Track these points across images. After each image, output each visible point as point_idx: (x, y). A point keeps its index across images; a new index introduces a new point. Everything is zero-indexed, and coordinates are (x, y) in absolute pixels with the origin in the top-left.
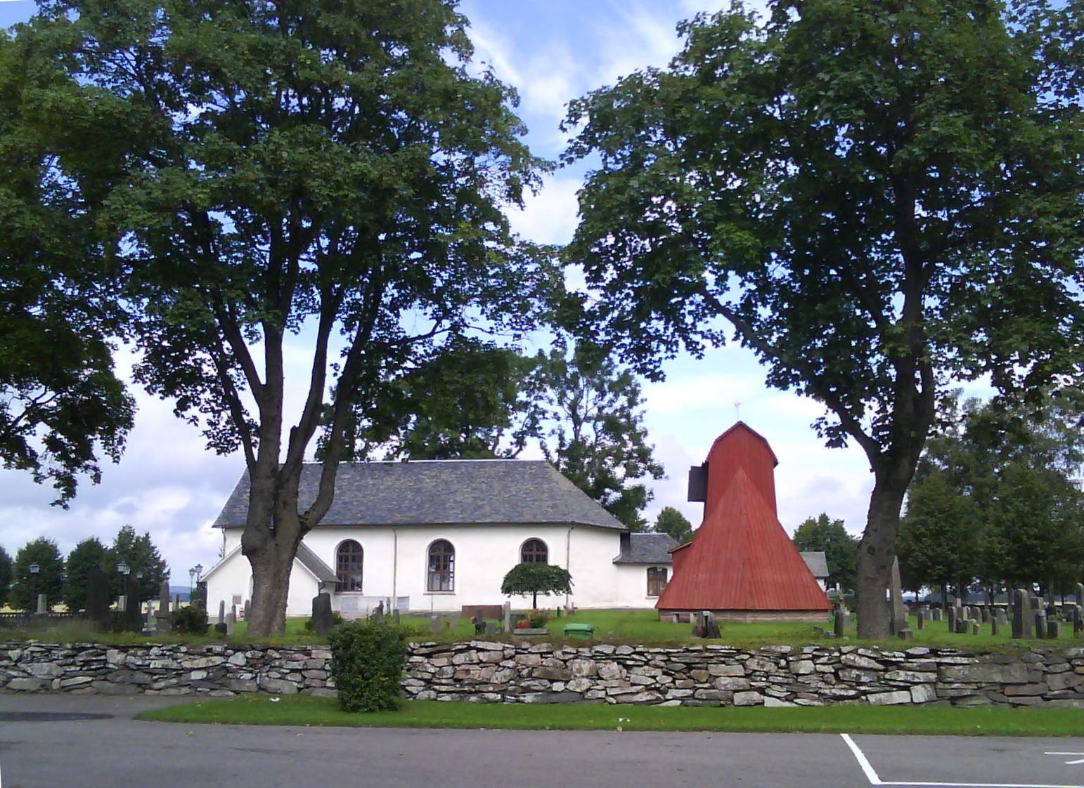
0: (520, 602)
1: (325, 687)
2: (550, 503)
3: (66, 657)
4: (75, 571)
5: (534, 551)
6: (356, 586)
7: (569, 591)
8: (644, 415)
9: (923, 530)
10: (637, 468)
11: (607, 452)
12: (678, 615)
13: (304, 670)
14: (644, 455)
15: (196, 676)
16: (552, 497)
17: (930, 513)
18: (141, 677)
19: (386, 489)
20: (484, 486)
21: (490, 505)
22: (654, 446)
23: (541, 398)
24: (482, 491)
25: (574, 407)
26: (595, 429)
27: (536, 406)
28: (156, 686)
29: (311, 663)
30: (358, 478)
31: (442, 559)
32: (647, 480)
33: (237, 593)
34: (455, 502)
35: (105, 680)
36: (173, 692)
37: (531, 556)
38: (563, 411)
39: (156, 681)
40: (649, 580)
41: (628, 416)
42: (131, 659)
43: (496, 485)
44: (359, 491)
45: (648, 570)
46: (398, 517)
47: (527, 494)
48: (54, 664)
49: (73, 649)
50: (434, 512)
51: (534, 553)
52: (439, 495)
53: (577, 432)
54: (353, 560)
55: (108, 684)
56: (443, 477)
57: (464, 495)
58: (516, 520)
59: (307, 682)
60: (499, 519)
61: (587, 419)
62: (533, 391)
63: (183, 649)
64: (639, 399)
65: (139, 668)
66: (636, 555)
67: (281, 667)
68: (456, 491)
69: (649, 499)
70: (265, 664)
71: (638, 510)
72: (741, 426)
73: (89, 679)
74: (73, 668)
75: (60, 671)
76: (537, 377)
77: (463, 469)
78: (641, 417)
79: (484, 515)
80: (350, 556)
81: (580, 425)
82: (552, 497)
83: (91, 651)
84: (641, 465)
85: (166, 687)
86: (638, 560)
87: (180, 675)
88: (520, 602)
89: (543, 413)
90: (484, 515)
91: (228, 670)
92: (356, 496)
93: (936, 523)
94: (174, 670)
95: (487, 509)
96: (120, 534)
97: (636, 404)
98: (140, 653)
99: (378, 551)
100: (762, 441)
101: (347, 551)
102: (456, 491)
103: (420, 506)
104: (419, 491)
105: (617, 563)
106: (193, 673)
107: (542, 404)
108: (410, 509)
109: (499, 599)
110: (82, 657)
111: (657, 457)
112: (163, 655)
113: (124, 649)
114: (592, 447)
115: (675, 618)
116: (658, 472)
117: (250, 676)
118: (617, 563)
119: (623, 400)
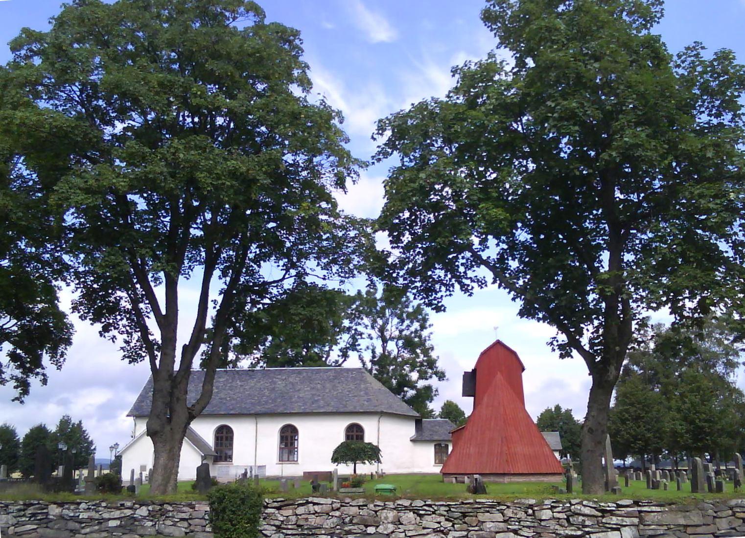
0: (345, 469)
1: (205, 531)
2: (366, 398)
3: (19, 510)
4: (27, 448)
5: (355, 433)
6: (228, 458)
7: (379, 461)
8: (431, 336)
9: (627, 416)
10: (426, 373)
11: (405, 362)
12: (456, 478)
13: (190, 519)
14: (431, 363)
15: (113, 524)
16: (366, 394)
17: (632, 405)
18: (73, 525)
20: (319, 386)
21: (323, 399)
22: (438, 357)
23: (360, 324)
24: (318, 390)
25: (382, 330)
26: (397, 345)
27: (356, 330)
28: (83, 531)
29: (195, 514)
31: (289, 438)
32: (434, 382)
33: (143, 463)
34: (299, 397)
35: (47, 527)
36: (95, 535)
37: (353, 436)
38: (375, 333)
39: (83, 528)
40: (436, 453)
41: (420, 337)
42: (66, 512)
43: (328, 385)
44: (231, 390)
45: (435, 445)
46: (258, 409)
47: (349, 391)
48: (10, 516)
49: (24, 504)
50: (284, 405)
51: (355, 434)
52: (287, 393)
53: (384, 348)
54: (227, 438)
55: (48, 530)
56: (291, 380)
57: (305, 392)
58: (342, 410)
59: (192, 528)
60: (330, 409)
61: (392, 339)
62: (354, 319)
63: (104, 504)
64: (428, 324)
65: (72, 518)
66: (426, 434)
67: (173, 517)
68: (299, 390)
69: (435, 395)
70: (161, 515)
71: (428, 402)
72: (498, 343)
73: (35, 527)
74: (24, 519)
75: (15, 521)
76: (357, 309)
77: (305, 374)
78: (429, 337)
79: (319, 407)
80: (224, 436)
81: (387, 342)
82: (366, 394)
83: (37, 506)
84: (430, 371)
85: (91, 532)
86: (427, 439)
87: (101, 523)
88: (345, 469)
89: (361, 334)
90: (319, 407)
91: (135, 519)
93: (636, 411)
94: (97, 520)
95: (322, 403)
96: (61, 421)
97: (426, 328)
98: (72, 507)
99: (243, 432)
100: (514, 353)
101: (222, 433)
102: (299, 390)
103: (274, 400)
104: (274, 389)
105: (413, 441)
106: (110, 522)
107: (360, 329)
108: (266, 402)
109: (330, 467)
110: (30, 511)
111: (440, 365)
112: (89, 509)
113: (61, 505)
114: (395, 358)
115: (454, 480)
116: (441, 376)
117: (150, 523)
118: (413, 441)
119: (416, 325)
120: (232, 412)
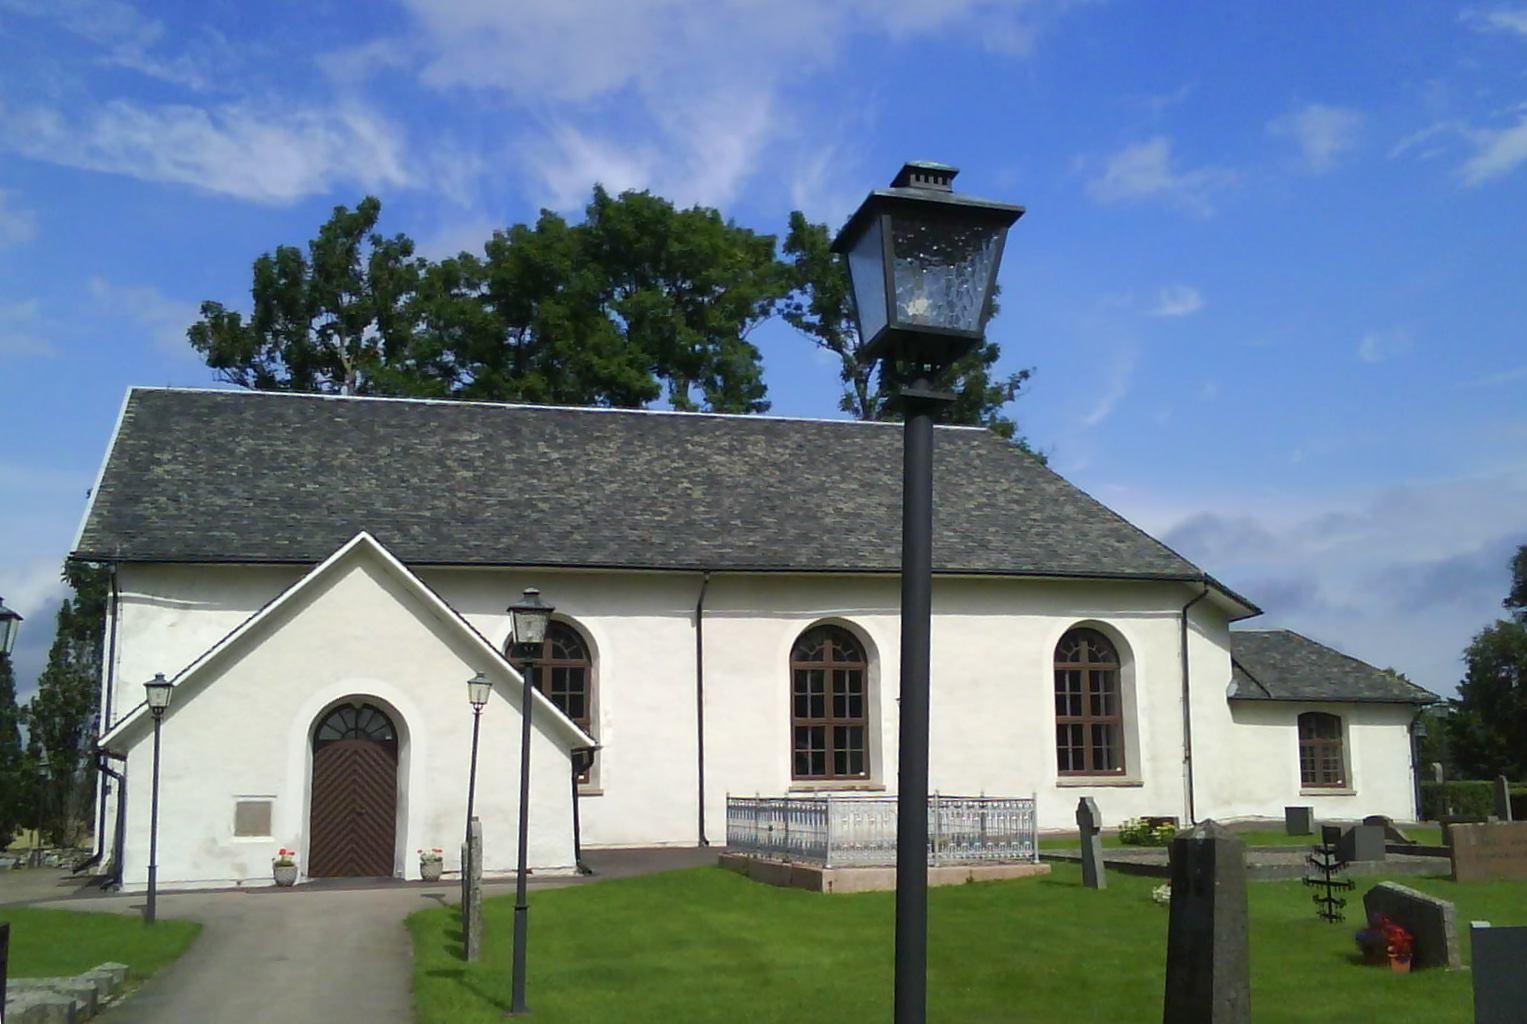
19: (611, 472)
30: (506, 443)
33: (252, 789)
44: (533, 474)
46: (703, 549)
51: (1084, 665)
92: (533, 488)
120: (595, 558)
